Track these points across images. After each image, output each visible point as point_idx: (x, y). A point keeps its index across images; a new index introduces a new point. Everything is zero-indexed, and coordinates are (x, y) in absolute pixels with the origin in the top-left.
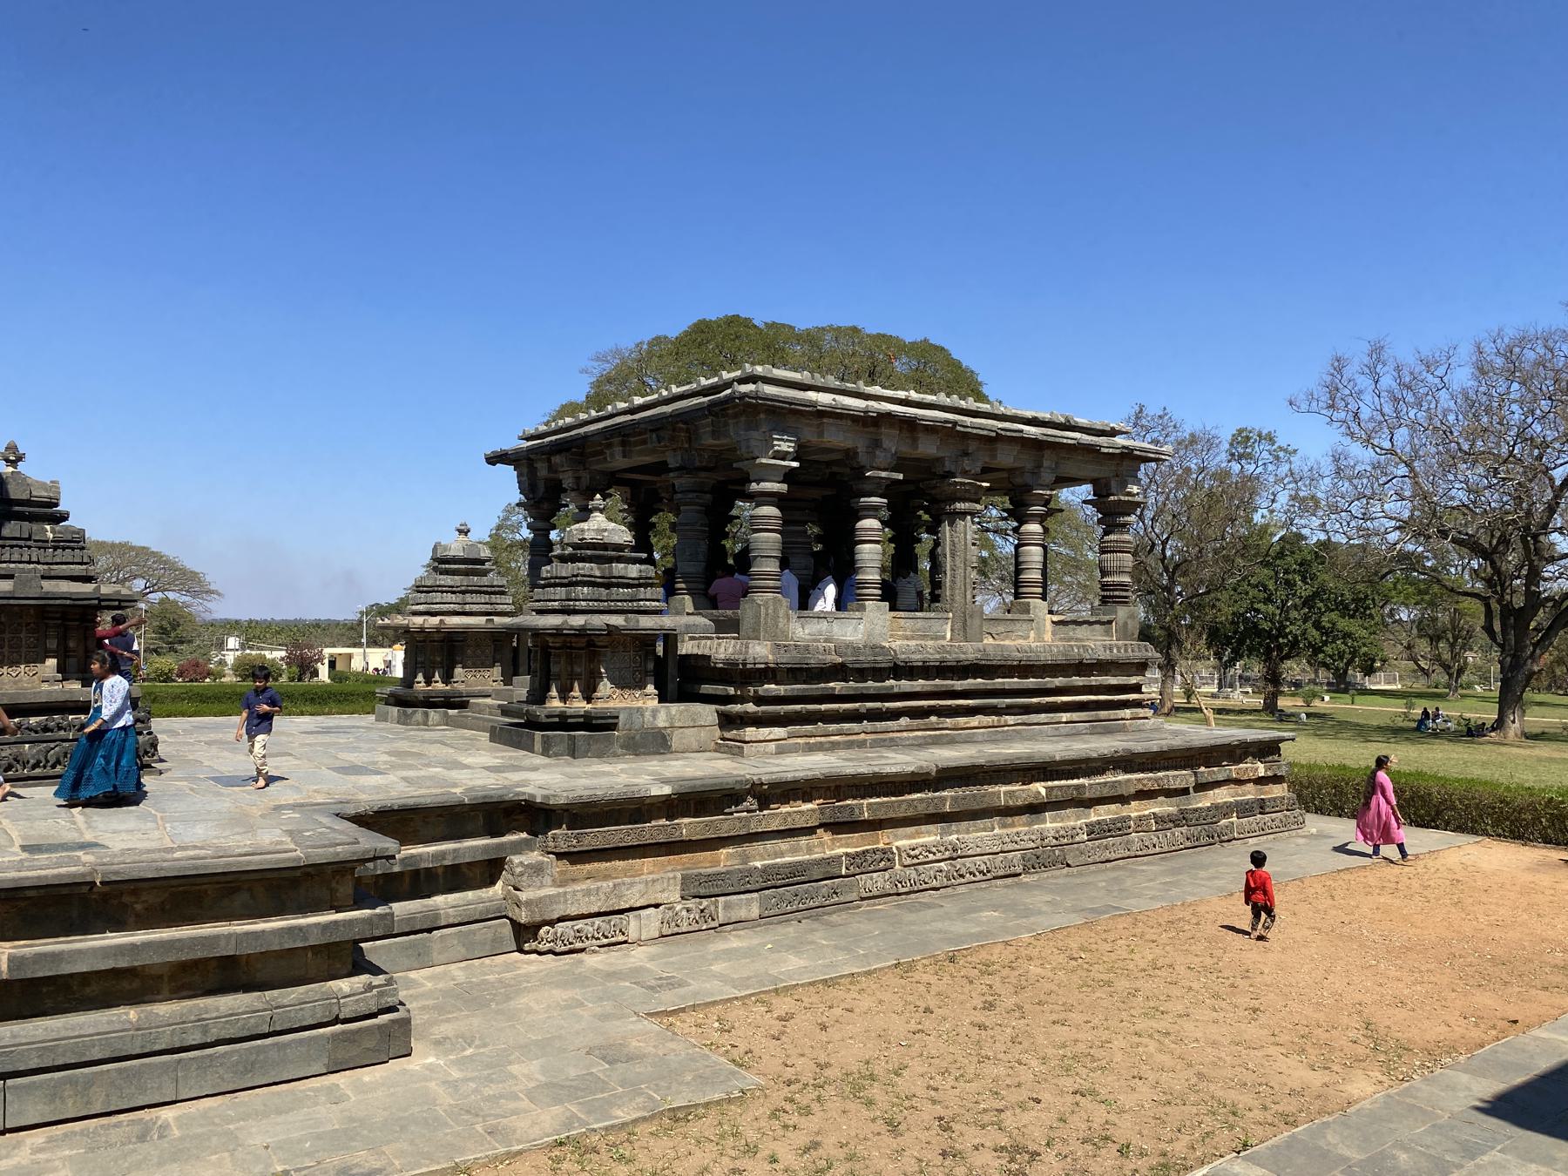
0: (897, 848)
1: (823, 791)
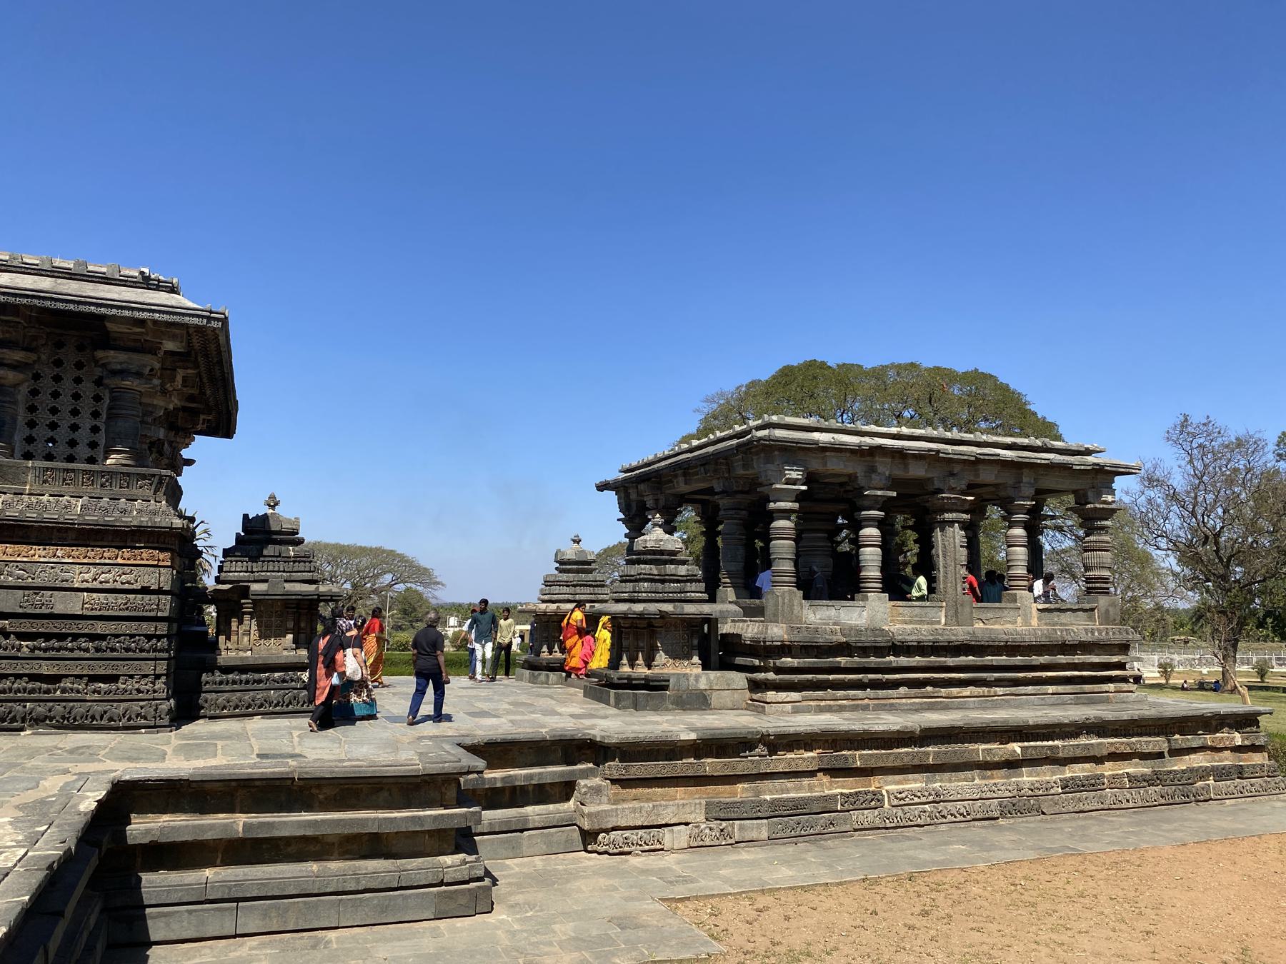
0: (887, 791)
1: (821, 743)
